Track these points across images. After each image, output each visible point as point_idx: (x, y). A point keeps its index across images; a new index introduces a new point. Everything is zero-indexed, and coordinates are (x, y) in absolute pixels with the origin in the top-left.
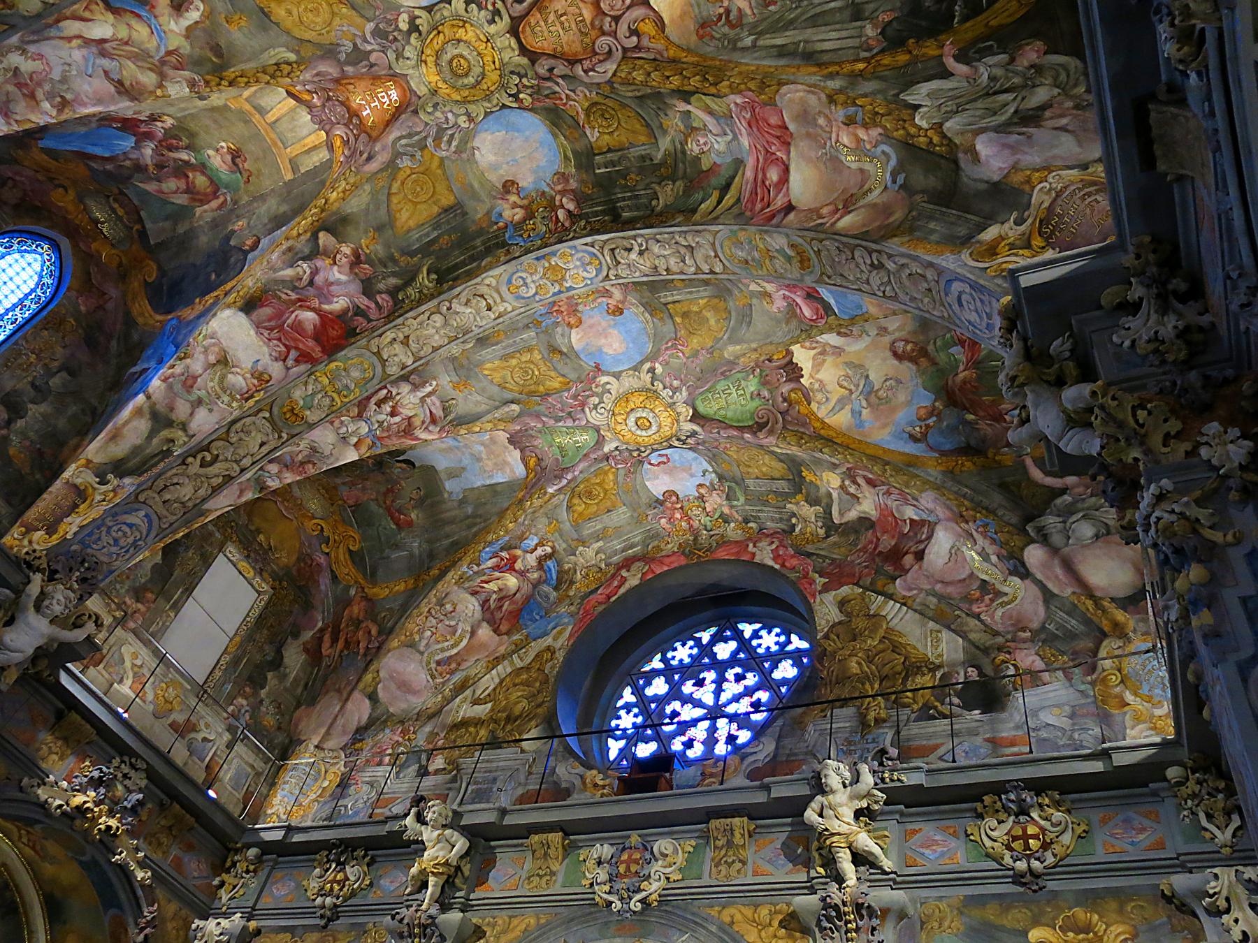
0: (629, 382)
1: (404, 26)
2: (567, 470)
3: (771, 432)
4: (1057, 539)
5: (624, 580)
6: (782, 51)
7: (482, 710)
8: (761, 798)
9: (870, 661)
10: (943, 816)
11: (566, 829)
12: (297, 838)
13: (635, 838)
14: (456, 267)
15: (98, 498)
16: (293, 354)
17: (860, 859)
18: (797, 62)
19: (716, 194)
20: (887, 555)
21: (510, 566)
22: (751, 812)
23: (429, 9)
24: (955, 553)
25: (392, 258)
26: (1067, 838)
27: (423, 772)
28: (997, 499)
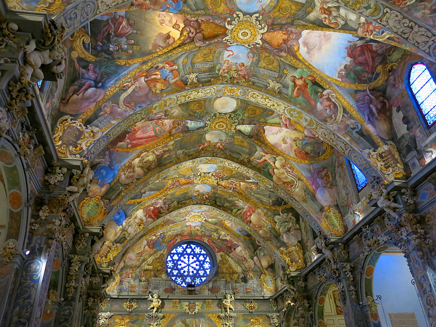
0: (196, 214)
1: (199, 174)
2: (176, 222)
3: (217, 226)
4: (258, 255)
5: (177, 240)
6: (258, 199)
7: (151, 267)
8: (215, 298)
9: (227, 270)
10: (240, 302)
11: (179, 299)
12: (120, 297)
13: (192, 301)
14: (182, 201)
15: (113, 249)
16: (148, 215)
17: (230, 309)
18: (259, 201)
19: (237, 210)
20: (229, 248)
21: (155, 235)
22: (212, 299)
23: (204, 173)
24: (241, 251)
25: (171, 199)
26: (256, 307)
27: (140, 281)
28: (251, 246)
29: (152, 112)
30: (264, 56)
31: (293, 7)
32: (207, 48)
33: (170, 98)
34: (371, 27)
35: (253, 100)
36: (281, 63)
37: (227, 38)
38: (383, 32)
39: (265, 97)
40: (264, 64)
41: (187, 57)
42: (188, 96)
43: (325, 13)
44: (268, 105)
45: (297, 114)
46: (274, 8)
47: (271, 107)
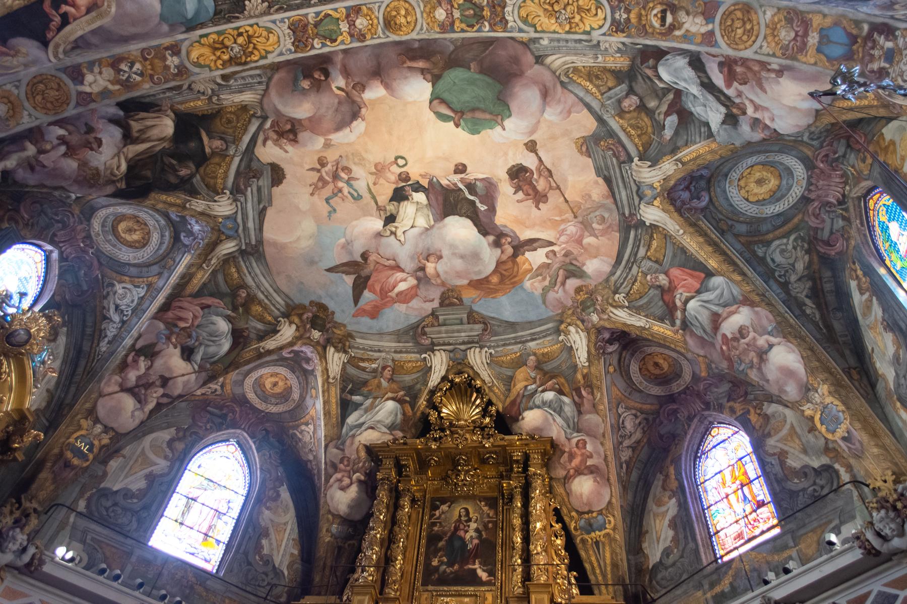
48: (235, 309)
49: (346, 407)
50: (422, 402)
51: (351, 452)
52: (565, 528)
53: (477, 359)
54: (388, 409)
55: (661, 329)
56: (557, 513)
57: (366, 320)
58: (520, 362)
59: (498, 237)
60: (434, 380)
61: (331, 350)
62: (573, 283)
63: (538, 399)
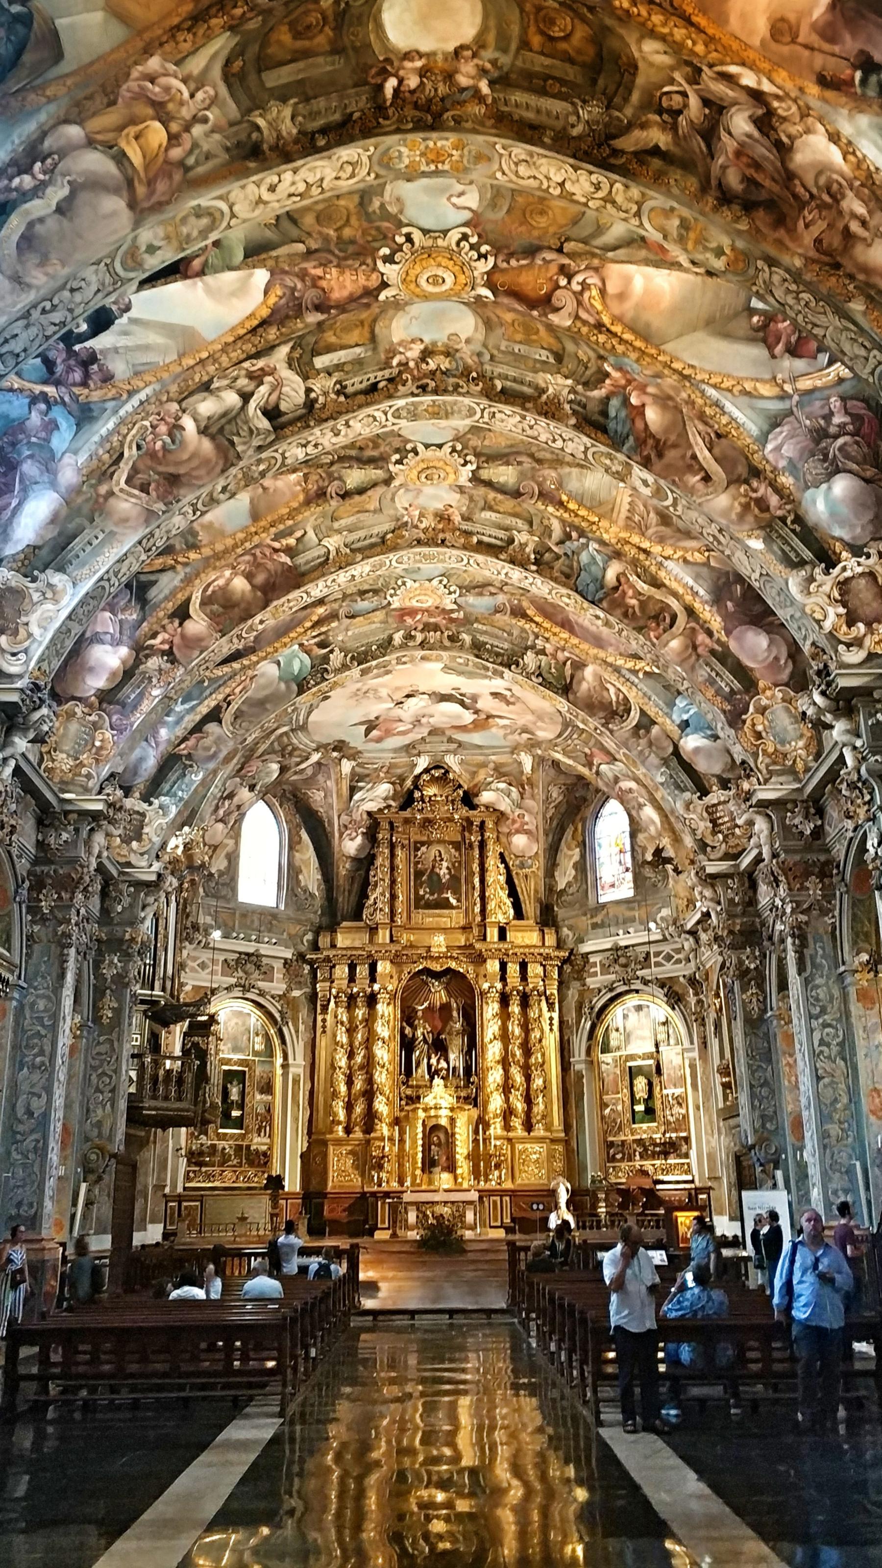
29: (733, 249)
30: (354, 221)
31: (333, 339)
32: (536, 233)
33: (665, 237)
34: (163, 428)
35: (346, 153)
36: (294, 232)
37: (483, 267)
38: (139, 447)
39: (315, 191)
40: (342, 202)
41: (600, 230)
42: (600, 194)
43: (262, 369)
44: (288, 176)
45: (188, 236)
46: (375, 321)
47: (275, 179)
48: (283, 756)
49: (353, 790)
50: (409, 783)
51: (356, 816)
52: (507, 867)
53: (451, 761)
54: (384, 789)
55: (585, 771)
56: (502, 856)
57: (372, 746)
58: (484, 765)
59: (477, 712)
60: (418, 770)
61: (344, 761)
62: (525, 736)
63: (493, 786)
